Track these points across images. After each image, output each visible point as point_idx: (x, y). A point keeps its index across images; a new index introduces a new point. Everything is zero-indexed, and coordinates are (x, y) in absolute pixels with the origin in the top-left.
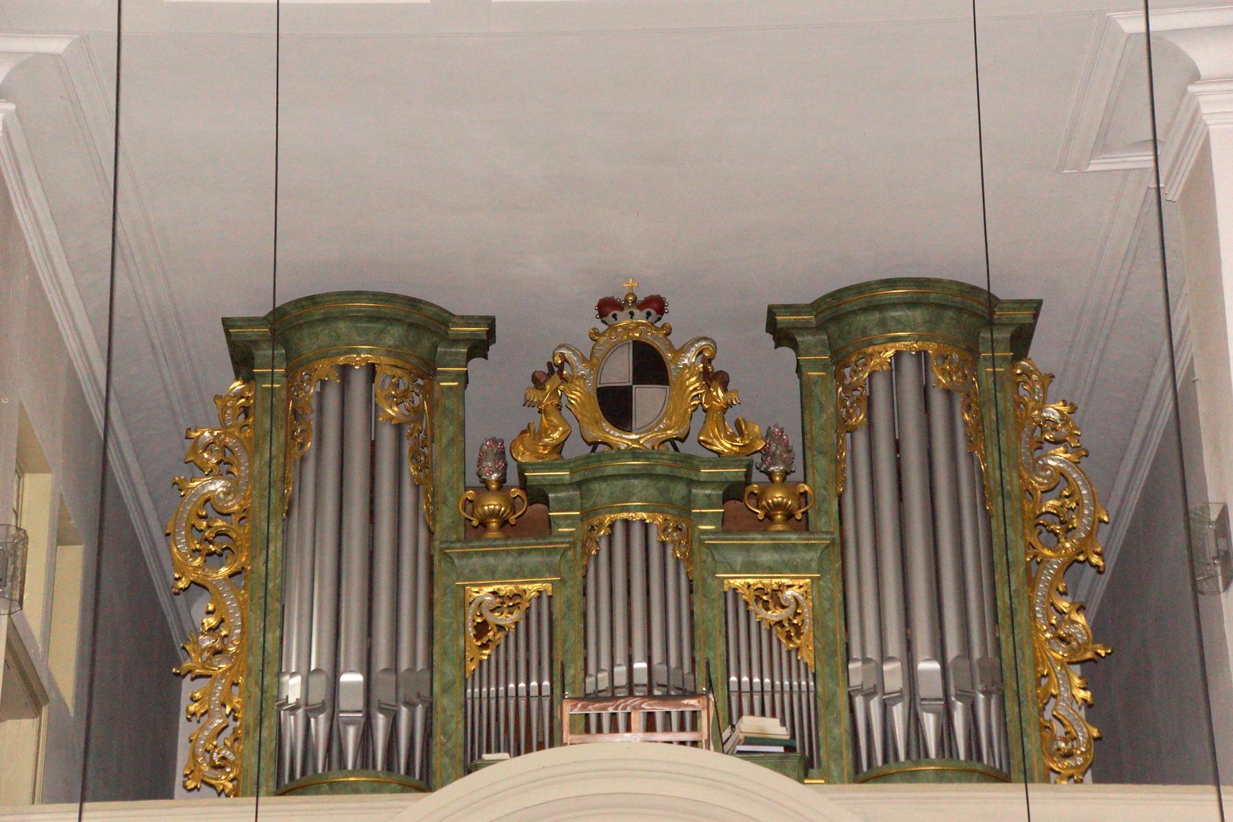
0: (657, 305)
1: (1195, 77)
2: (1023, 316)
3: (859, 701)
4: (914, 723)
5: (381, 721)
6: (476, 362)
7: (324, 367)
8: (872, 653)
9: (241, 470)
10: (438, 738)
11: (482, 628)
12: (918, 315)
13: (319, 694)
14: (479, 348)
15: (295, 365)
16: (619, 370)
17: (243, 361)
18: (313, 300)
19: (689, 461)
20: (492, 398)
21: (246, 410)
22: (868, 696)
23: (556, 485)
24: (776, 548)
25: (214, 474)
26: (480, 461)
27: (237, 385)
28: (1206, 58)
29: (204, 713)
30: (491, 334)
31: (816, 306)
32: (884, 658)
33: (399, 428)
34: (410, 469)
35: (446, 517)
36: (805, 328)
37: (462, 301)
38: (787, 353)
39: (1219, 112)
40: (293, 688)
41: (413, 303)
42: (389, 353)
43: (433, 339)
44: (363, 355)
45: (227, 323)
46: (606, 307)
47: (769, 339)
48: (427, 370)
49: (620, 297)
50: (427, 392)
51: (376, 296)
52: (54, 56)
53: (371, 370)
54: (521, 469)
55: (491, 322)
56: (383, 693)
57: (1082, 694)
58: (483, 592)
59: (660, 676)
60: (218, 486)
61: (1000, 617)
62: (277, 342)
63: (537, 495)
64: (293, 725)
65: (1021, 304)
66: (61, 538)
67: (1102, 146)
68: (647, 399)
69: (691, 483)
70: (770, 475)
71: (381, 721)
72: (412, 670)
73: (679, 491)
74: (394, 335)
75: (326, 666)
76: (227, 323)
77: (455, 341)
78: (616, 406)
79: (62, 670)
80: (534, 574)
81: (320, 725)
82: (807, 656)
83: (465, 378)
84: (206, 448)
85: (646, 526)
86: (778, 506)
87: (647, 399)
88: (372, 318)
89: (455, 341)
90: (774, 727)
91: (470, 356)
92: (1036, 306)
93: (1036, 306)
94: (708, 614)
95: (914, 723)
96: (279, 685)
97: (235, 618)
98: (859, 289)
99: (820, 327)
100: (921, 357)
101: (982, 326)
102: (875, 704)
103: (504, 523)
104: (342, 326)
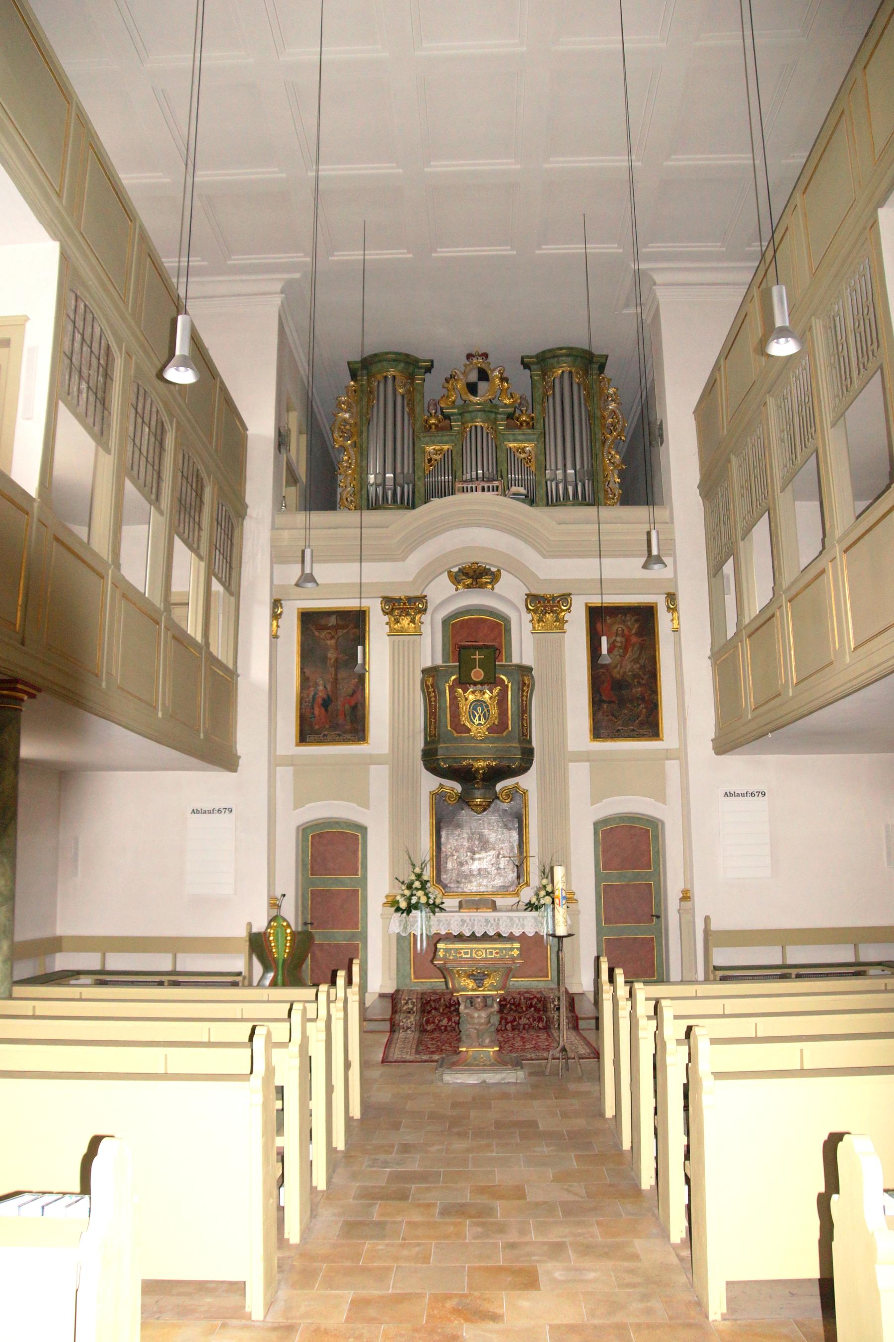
0: (485, 355)
1: (655, 284)
2: (603, 360)
3: (549, 483)
4: (566, 490)
5: (399, 489)
6: (427, 375)
7: (380, 377)
8: (553, 467)
9: (354, 410)
10: (417, 494)
11: (430, 460)
12: (570, 359)
13: (380, 481)
14: (428, 370)
15: (370, 376)
16: (473, 377)
17: (354, 376)
18: (375, 355)
19: (496, 406)
20: (432, 386)
21: (355, 391)
22: (552, 481)
23: (453, 414)
24: (523, 434)
25: (346, 412)
26: (429, 406)
27: (352, 383)
28: (658, 278)
29: (345, 486)
30: (432, 366)
31: (537, 356)
32: (557, 469)
33: (403, 396)
34: (407, 410)
35: (418, 426)
36: (533, 363)
37: (422, 354)
38: (527, 372)
39: (662, 295)
40: (372, 478)
41: (408, 356)
42: (399, 371)
43: (414, 367)
44: (392, 372)
45: (349, 363)
46: (469, 356)
47: (522, 367)
48: (411, 377)
49: (474, 353)
50: (412, 384)
51: (396, 353)
52: (296, 279)
53: (394, 378)
54: (442, 409)
55: (432, 362)
56: (400, 480)
57: (618, 480)
58: (430, 449)
59: (486, 475)
60: (347, 416)
61: (593, 456)
62: (364, 368)
63: (447, 417)
64: (372, 490)
65: (602, 356)
66: (300, 432)
67: (627, 306)
68: (482, 386)
69: (496, 413)
70: (522, 411)
71: (399, 489)
72: (408, 473)
73: (493, 416)
74: (401, 365)
75: (382, 472)
76: (349, 363)
77: (420, 368)
78: (472, 389)
79: (302, 472)
80: (446, 443)
81: (380, 490)
82: (533, 469)
83: (424, 380)
84: (343, 403)
85: (482, 428)
86: (525, 421)
87: (482, 386)
88: (394, 361)
89: (420, 368)
90: (522, 490)
91: (426, 372)
92: (607, 356)
93: (607, 356)
94: (502, 455)
95: (566, 490)
96: (367, 478)
97: (353, 457)
98: (550, 351)
99: (537, 363)
100: (570, 372)
101: (590, 363)
102: (554, 484)
103: (436, 426)
104: (385, 363)
